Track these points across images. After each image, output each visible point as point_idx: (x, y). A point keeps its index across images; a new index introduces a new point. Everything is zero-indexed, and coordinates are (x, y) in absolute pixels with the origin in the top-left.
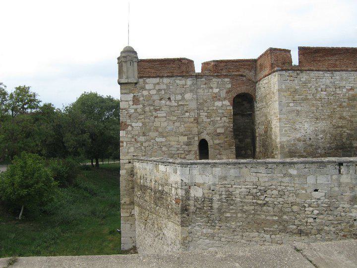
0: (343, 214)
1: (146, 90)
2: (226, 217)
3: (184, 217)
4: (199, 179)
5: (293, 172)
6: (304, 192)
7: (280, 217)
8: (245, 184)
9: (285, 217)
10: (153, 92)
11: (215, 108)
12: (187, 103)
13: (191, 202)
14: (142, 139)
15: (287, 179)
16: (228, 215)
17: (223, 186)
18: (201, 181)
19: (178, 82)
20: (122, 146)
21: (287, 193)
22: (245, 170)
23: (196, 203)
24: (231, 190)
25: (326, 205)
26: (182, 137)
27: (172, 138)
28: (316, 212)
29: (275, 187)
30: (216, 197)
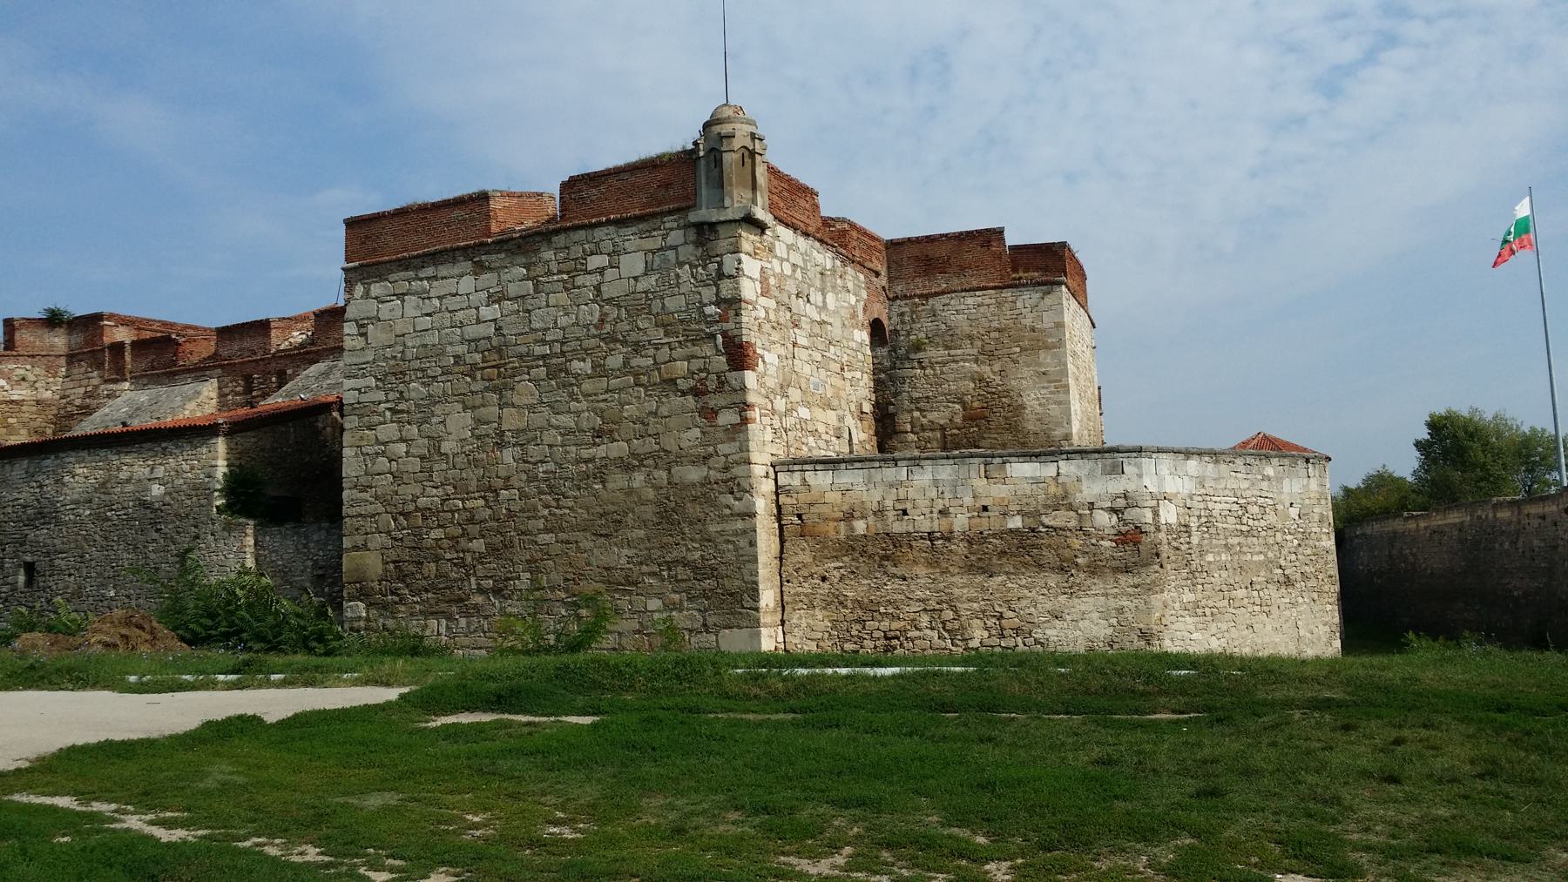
0: (1317, 543)
1: (776, 257)
2: (1210, 563)
3: (1156, 572)
4: (1173, 485)
5: (1269, 471)
6: (1282, 507)
7: (1266, 556)
8: (1227, 492)
9: (1270, 555)
10: (788, 270)
11: (854, 345)
12: (831, 320)
13: (1162, 536)
14: (780, 404)
15: (1265, 485)
16: (1210, 558)
17: (1200, 499)
18: (1175, 491)
19: (815, 253)
20: (754, 421)
21: (1267, 509)
22: (1223, 467)
23: (1169, 537)
24: (1211, 505)
25: (1302, 530)
26: (830, 412)
27: (819, 413)
28: (1296, 542)
29: (1254, 499)
30: (1194, 523)
